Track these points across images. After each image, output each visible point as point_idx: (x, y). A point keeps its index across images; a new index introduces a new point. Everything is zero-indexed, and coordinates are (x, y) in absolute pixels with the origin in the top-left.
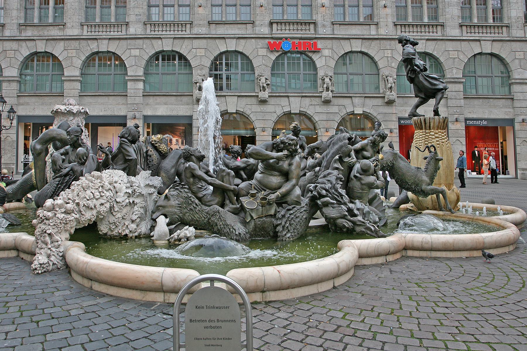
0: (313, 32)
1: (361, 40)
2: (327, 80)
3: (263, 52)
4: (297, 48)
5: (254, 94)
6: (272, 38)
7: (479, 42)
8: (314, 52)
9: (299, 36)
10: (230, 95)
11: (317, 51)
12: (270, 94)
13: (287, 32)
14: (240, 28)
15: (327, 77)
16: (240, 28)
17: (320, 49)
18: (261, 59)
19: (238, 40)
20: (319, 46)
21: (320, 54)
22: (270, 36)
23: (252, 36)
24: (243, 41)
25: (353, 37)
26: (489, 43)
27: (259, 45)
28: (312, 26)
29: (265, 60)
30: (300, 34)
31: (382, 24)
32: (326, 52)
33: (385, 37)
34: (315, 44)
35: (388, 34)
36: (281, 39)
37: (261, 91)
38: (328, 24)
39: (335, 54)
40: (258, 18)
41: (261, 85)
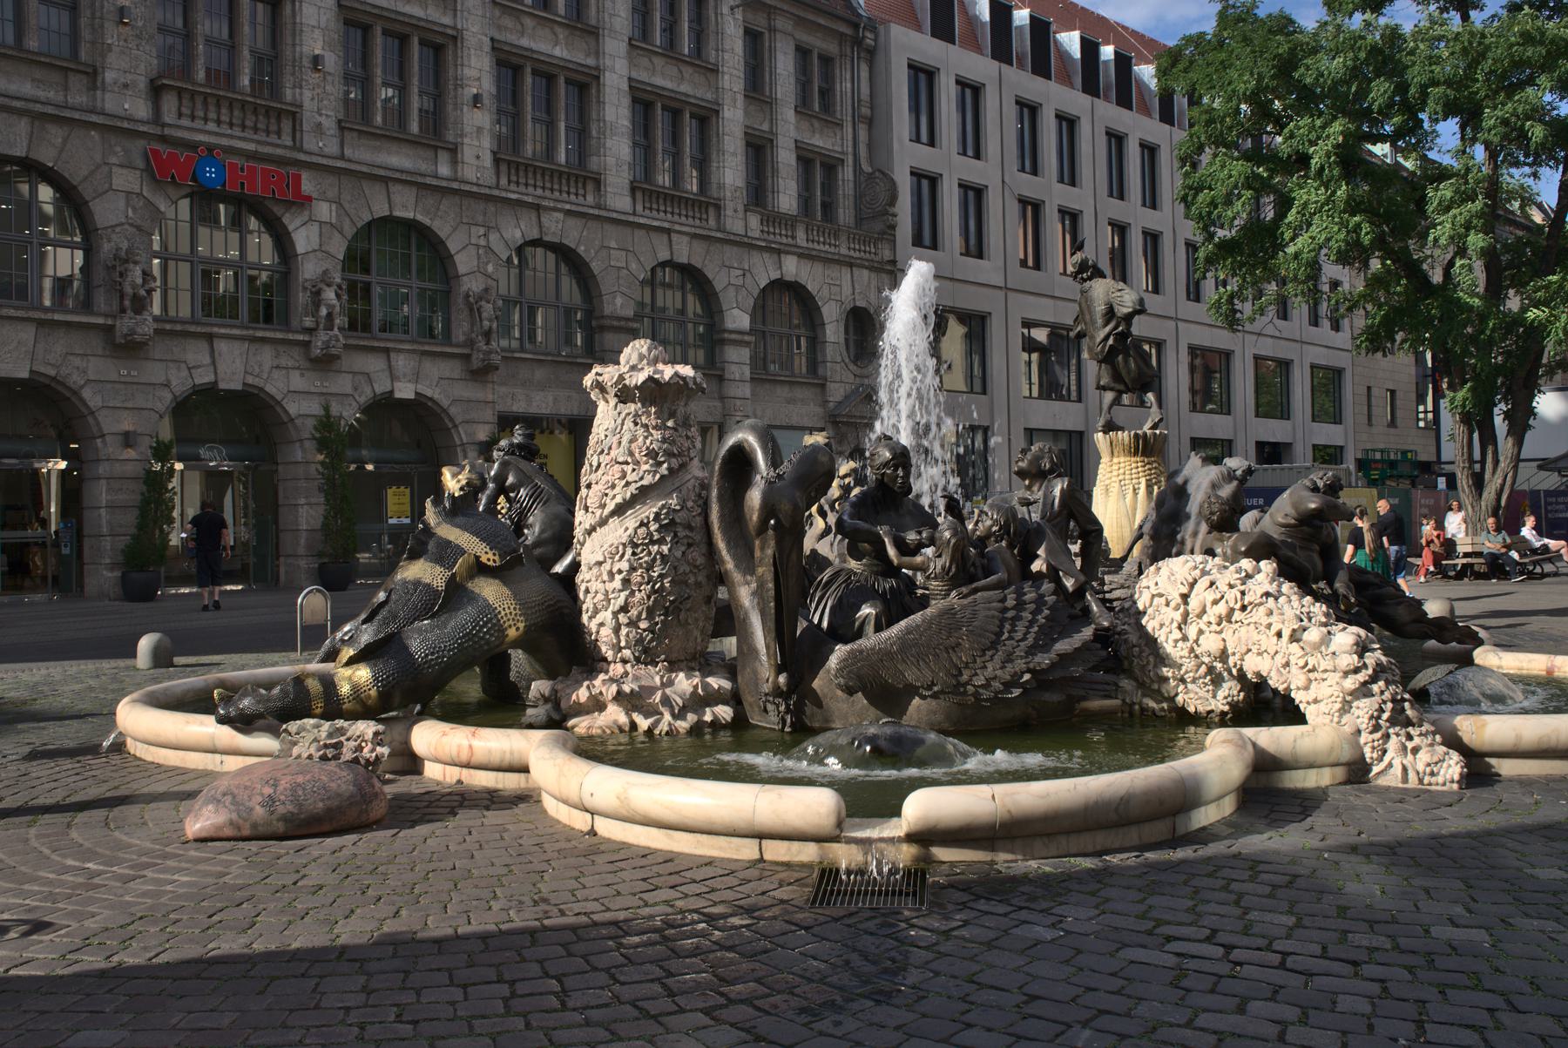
0: (289, 143)
1: (414, 190)
2: (330, 295)
3: (127, 180)
4: (243, 184)
5: (100, 321)
6: (163, 139)
7: (665, 237)
8: (289, 205)
9: (251, 147)
10: (17, 318)
11: (302, 202)
12: (160, 326)
13: (211, 126)
14: (39, 81)
15: (329, 285)
16: (39, 81)
17: (309, 199)
18: (122, 204)
19: (37, 123)
20: (307, 186)
21: (307, 213)
22: (158, 131)
23: (94, 118)
24: (56, 134)
25: (397, 175)
26: (686, 239)
27: (115, 153)
28: (286, 126)
29: (134, 209)
30: (252, 141)
31: (468, 154)
32: (324, 210)
33: (475, 189)
34: (298, 179)
35: (481, 182)
36: (193, 146)
37: (123, 311)
38: (329, 124)
39: (347, 220)
40: (112, 59)
41: (128, 290)
